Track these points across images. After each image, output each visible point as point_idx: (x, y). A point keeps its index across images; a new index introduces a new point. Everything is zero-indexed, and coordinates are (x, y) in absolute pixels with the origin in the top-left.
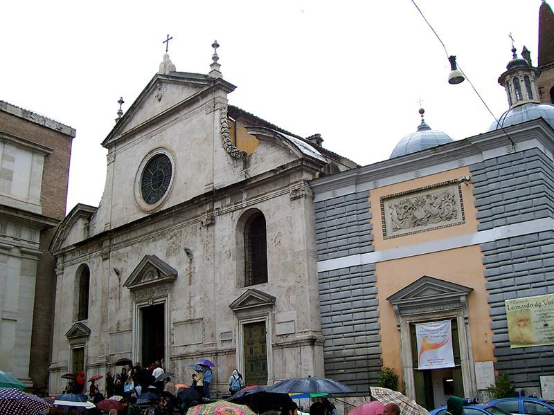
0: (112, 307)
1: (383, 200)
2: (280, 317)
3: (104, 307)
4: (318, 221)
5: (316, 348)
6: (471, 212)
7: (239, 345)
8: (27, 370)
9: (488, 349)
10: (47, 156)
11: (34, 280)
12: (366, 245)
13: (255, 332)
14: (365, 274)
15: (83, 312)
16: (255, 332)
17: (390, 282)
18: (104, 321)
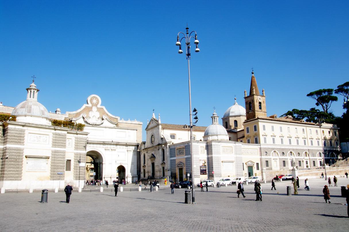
0: (148, 162)
1: (177, 149)
2: (166, 166)
3: (147, 162)
4: (170, 151)
5: (169, 171)
6: (185, 153)
7: (162, 170)
8: (136, 173)
9: (185, 172)
10: (137, 130)
11: (136, 156)
12: (175, 156)
13: (163, 168)
14: (174, 160)
15: (145, 163)
16: (163, 168)
17: (177, 162)
18: (147, 165)
